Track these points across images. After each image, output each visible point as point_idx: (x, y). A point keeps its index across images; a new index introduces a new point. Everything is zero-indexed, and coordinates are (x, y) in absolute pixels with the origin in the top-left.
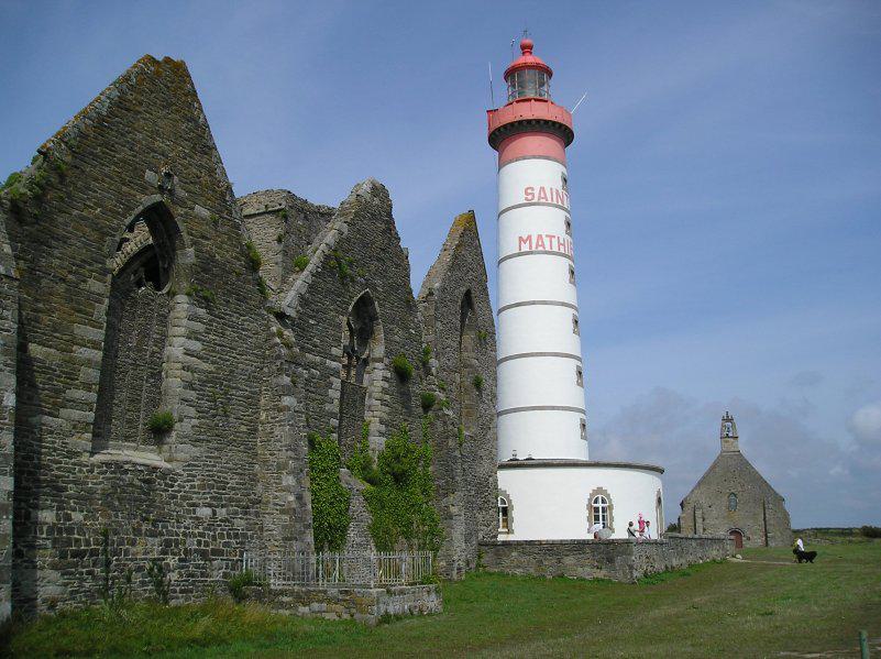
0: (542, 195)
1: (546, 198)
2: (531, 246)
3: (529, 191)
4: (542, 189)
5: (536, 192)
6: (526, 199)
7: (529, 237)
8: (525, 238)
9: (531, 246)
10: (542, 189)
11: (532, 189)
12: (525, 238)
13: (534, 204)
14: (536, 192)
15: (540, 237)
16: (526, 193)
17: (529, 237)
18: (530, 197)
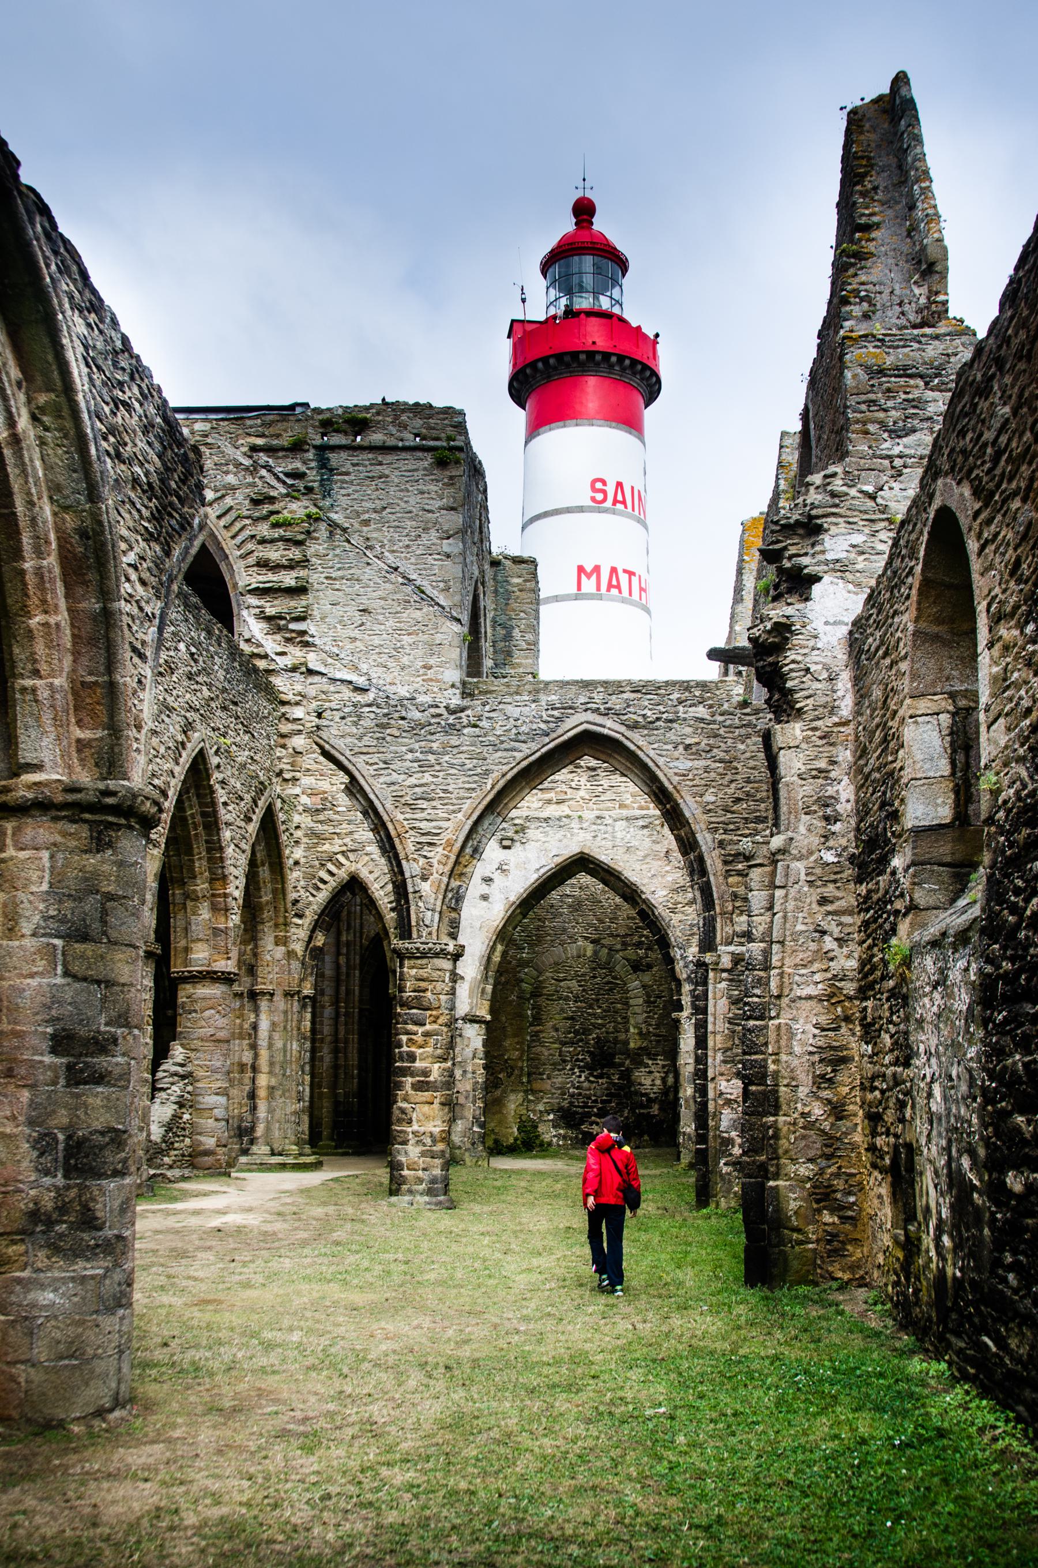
0: (620, 498)
1: (624, 502)
2: (598, 588)
3: (599, 485)
4: (619, 485)
5: (610, 489)
6: (593, 499)
7: (597, 569)
8: (589, 569)
9: (598, 588)
10: (619, 485)
11: (604, 483)
12: (589, 569)
13: (606, 511)
14: (610, 489)
15: (614, 570)
16: (594, 489)
17: (597, 569)
18: (599, 497)
